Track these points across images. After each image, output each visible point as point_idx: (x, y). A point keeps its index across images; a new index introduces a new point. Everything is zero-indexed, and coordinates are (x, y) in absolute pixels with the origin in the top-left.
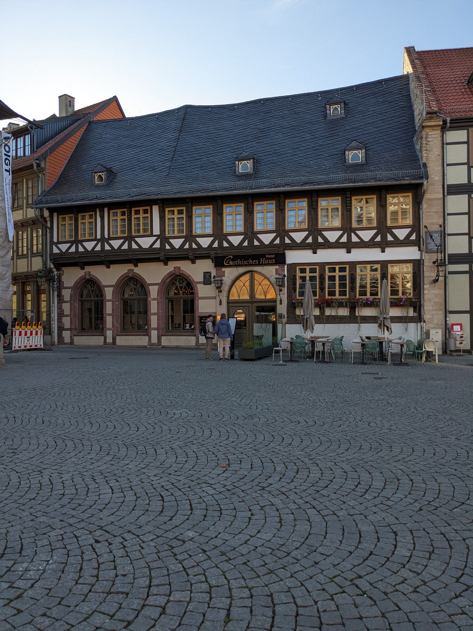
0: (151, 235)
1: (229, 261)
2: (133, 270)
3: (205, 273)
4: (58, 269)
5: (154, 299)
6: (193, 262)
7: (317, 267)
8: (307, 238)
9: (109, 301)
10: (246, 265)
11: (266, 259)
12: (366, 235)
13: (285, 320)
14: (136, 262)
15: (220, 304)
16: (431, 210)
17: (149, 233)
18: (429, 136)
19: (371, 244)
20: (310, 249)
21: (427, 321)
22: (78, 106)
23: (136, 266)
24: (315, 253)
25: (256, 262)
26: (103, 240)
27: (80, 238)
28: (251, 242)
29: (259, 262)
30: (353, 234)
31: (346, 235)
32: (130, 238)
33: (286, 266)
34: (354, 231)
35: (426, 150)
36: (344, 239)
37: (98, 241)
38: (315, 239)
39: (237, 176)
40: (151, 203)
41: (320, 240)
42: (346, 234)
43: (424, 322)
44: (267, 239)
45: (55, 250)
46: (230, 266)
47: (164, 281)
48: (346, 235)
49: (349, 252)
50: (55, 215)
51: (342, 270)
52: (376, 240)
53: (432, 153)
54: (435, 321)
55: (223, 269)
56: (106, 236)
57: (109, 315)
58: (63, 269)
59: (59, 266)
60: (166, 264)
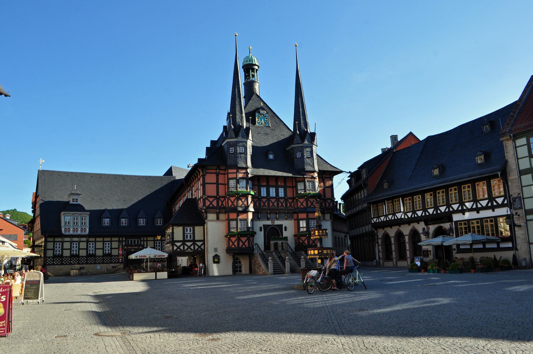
0: (401, 212)
2: (399, 229)
3: (423, 228)
4: (376, 230)
5: (407, 243)
6: (419, 223)
7: (493, 219)
8: (458, 207)
9: (393, 244)
11: (444, 219)
12: (484, 203)
13: (456, 251)
14: (399, 225)
16: (513, 186)
17: (399, 211)
18: (507, 145)
19: (486, 208)
20: (460, 213)
21: (519, 249)
22: (399, 139)
23: (400, 227)
26: (386, 216)
27: (379, 215)
28: (437, 212)
30: (478, 203)
31: (475, 204)
32: (394, 214)
33: (453, 223)
34: (478, 201)
35: (506, 153)
37: (385, 216)
38: (462, 208)
39: (434, 177)
40: (398, 197)
41: (465, 208)
42: (475, 203)
43: (517, 250)
44: (443, 209)
45: (373, 222)
47: (410, 233)
48: (475, 204)
49: (478, 212)
50: (371, 205)
51: (477, 223)
52: (489, 205)
53: (510, 153)
54: (523, 249)
55: (429, 226)
56: (387, 214)
57: (394, 251)
58: (378, 230)
59: (376, 229)
60: (409, 225)
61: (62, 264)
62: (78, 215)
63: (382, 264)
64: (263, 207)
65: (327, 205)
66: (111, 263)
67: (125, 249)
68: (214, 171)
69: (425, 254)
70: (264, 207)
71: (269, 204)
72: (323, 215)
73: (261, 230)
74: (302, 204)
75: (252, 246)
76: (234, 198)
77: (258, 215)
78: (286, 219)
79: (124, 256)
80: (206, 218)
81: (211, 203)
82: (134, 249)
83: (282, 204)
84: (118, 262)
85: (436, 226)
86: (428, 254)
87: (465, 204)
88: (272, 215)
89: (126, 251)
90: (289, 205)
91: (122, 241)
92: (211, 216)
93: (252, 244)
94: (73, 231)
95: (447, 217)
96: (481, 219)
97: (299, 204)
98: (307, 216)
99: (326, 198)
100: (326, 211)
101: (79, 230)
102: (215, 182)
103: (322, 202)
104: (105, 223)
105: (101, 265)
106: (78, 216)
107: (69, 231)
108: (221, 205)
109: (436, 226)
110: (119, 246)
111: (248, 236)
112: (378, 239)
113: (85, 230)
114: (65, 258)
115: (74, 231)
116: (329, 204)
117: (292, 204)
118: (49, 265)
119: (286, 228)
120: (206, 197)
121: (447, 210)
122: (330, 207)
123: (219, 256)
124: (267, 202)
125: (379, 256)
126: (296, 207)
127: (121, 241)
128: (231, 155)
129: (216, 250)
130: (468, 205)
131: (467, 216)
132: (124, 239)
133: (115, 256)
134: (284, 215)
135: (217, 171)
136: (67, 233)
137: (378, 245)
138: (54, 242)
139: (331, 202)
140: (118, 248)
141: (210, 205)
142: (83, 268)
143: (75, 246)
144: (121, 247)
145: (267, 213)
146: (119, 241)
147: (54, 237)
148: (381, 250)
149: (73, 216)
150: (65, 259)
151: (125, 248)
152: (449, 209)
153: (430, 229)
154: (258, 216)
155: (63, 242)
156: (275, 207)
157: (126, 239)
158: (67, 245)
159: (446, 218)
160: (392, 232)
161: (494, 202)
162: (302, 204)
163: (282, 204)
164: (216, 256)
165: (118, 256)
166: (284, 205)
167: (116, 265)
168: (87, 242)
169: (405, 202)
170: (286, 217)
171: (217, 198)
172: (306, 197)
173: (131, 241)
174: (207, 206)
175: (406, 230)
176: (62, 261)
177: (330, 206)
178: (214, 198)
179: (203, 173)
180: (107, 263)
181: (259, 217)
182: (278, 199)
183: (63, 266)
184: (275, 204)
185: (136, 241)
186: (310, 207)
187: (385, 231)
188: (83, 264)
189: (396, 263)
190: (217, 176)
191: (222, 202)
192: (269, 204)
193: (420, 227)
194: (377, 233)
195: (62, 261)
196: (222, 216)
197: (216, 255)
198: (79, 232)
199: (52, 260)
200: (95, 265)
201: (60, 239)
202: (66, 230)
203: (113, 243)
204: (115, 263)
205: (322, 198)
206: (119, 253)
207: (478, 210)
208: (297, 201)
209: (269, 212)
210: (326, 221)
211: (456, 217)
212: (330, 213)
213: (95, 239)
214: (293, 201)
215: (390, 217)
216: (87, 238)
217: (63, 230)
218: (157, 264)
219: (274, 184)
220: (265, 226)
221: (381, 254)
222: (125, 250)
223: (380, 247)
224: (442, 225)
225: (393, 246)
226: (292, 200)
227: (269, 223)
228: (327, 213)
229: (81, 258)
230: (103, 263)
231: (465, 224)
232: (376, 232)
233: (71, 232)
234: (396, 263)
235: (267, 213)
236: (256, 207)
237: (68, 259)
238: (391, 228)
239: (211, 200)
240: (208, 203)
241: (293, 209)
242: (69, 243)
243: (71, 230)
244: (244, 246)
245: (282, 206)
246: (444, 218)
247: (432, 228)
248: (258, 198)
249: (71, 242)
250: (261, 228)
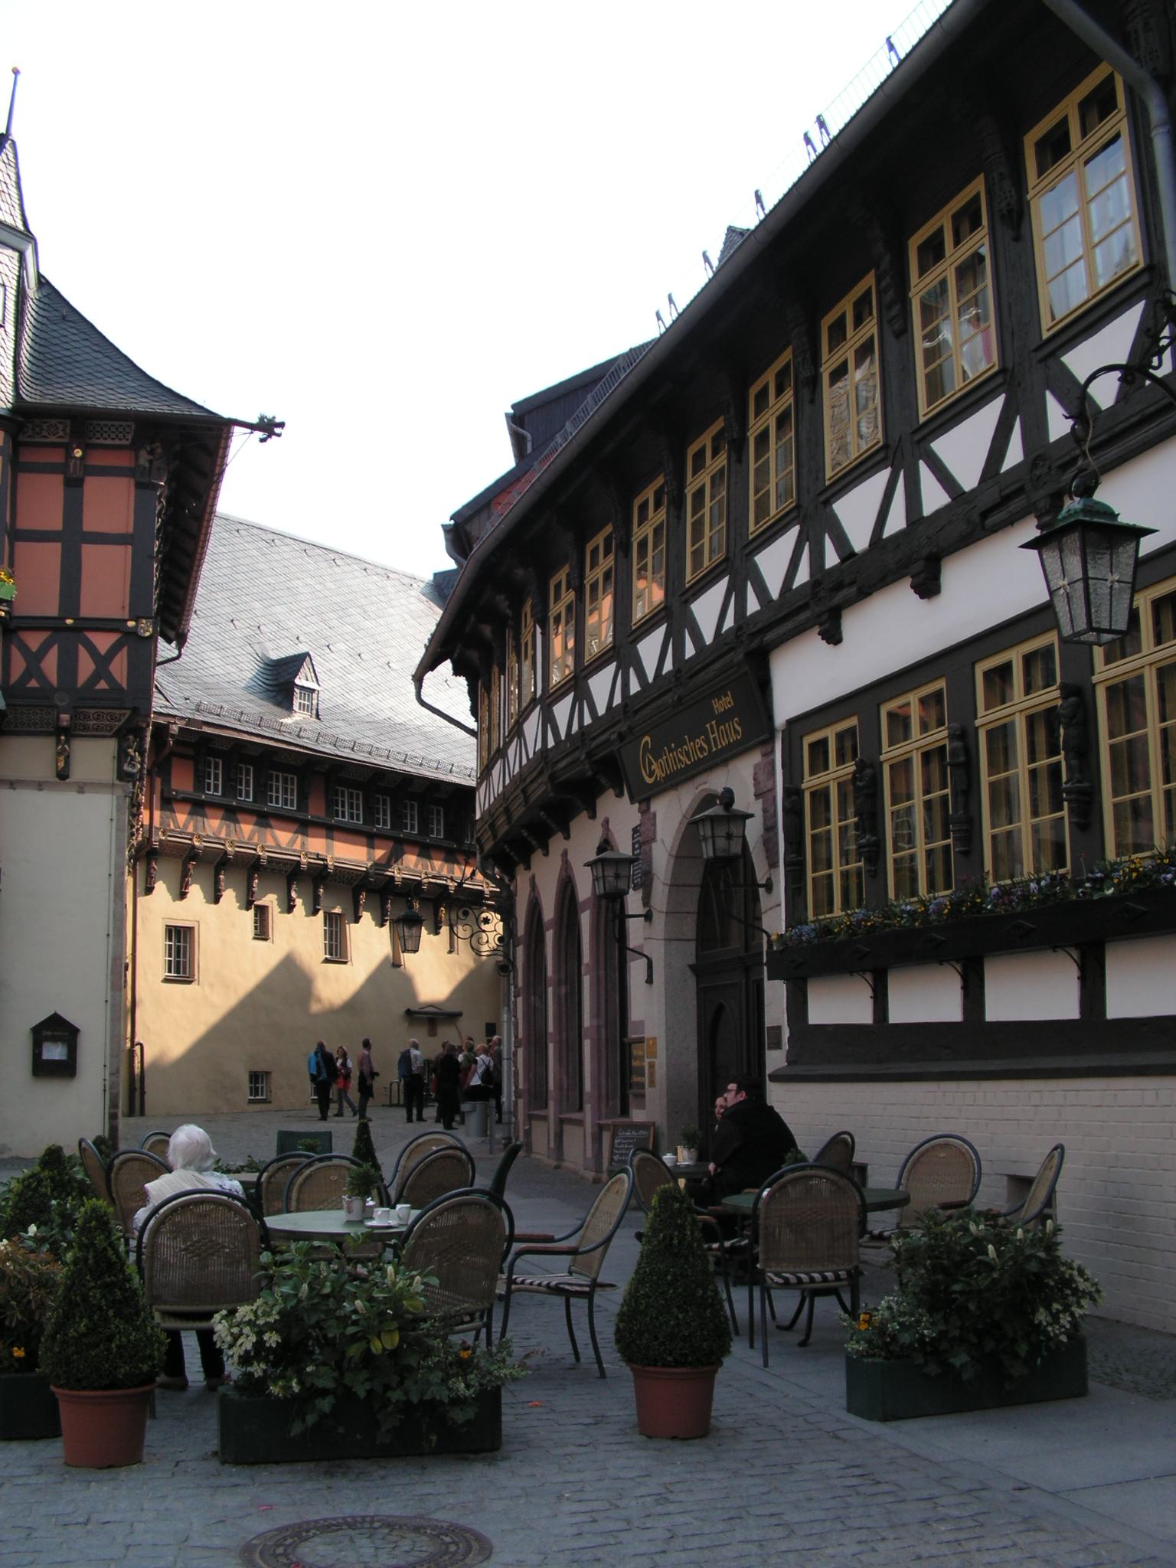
24: (833, 637)
49: (928, 587)
65: (86, 667)
103: (45, 648)
116: (103, 662)
122: (103, 685)
139: (114, 650)
153: (659, 837)
177: (110, 679)
212: (121, 735)
224: (716, 781)
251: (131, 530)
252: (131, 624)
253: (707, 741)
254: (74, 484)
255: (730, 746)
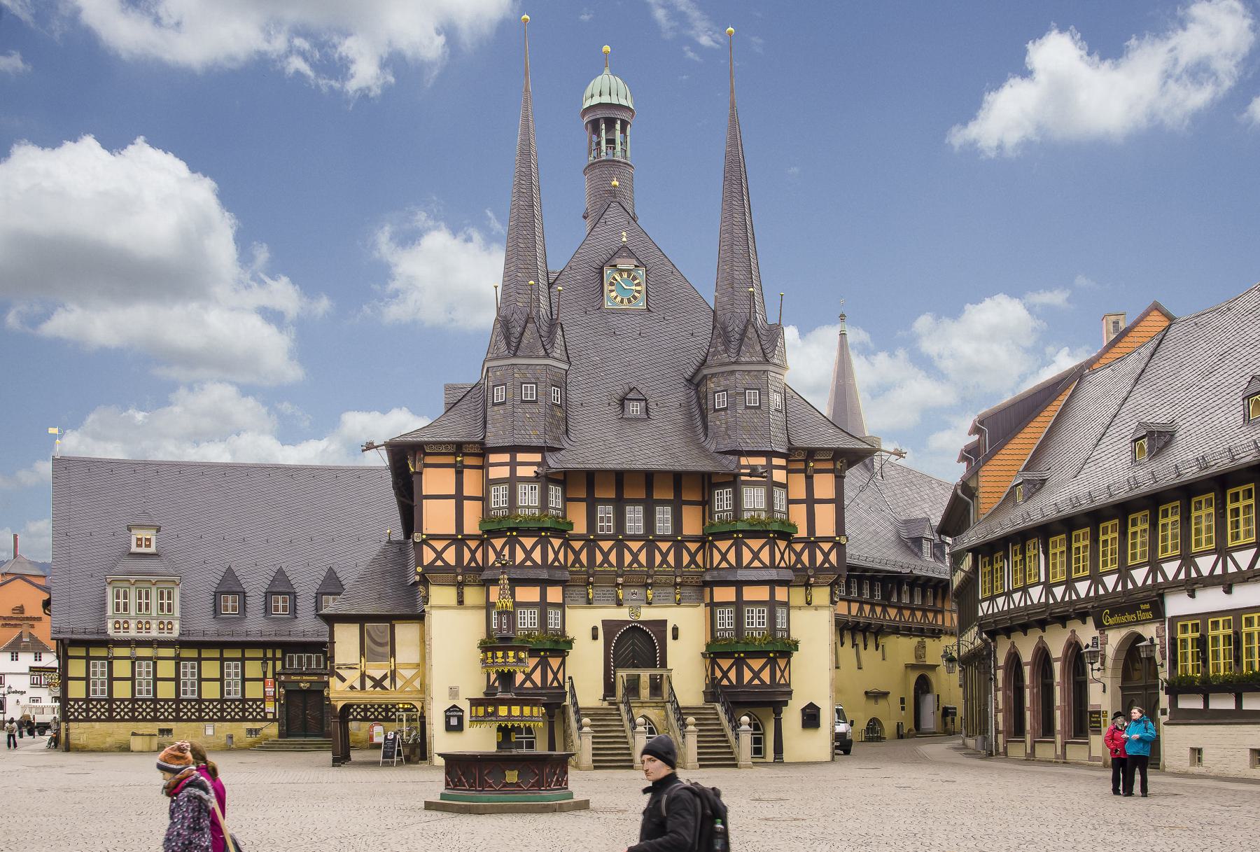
1: (1108, 618)
3: (1094, 638)
10: (1125, 623)
15: (1104, 691)
24: (1192, 595)
25: (1133, 618)
29: (1136, 616)
36: (1218, 571)
38: (1188, 573)
44: (1139, 575)
46: (1110, 627)
49: (1228, 591)
61: (111, 719)
62: (148, 585)
63: (1001, 750)
64: (601, 565)
65: (820, 558)
66: (243, 719)
67: (283, 682)
68: (450, 460)
69: (1094, 722)
70: (606, 565)
71: (620, 557)
72: (807, 589)
73: (595, 637)
74: (724, 557)
75: (555, 684)
76: (503, 540)
77: (587, 590)
78: (679, 603)
79: (279, 700)
80: (426, 599)
81: (439, 555)
82: (307, 682)
83: (665, 556)
84: (264, 719)
85: (1124, 632)
86: (1100, 722)
87: (1197, 560)
88: (632, 591)
89: (284, 688)
90: (686, 559)
91: (274, 659)
92: (441, 595)
93: (555, 678)
94: (138, 629)
95: (1152, 601)
96: (1237, 613)
97: (717, 557)
98: (739, 594)
99: (815, 538)
100: (812, 579)
101: (154, 626)
102: (453, 492)
104: (227, 606)
105: (217, 724)
106: (129, 588)
107: (128, 628)
108: (470, 562)
109: (1124, 632)
110: (265, 673)
111: (542, 653)
112: (996, 668)
113: (170, 627)
114: (162, 703)
115: (141, 628)
116: (826, 555)
117: (699, 558)
118: (76, 720)
119: (675, 629)
120: (424, 537)
121: (1149, 582)
122: (827, 565)
123: (462, 711)
124: (614, 551)
125: (997, 723)
126: (708, 567)
127: (269, 659)
128: (496, 408)
129: (454, 692)
130: (1205, 564)
131: (1211, 600)
132: (279, 655)
133: (254, 701)
134: (671, 590)
135: (459, 459)
136: (122, 635)
137: (997, 690)
138: (88, 658)
140: (263, 679)
141: (435, 560)
142: (169, 731)
143: (144, 669)
144: (270, 675)
145: (617, 585)
146: (265, 660)
147: (87, 644)
148: (1001, 706)
149: (114, 588)
150: (119, 707)
151: (283, 678)
152: (1188, 573)
154: (588, 594)
155: (110, 661)
156: (640, 565)
157: (284, 655)
158: (121, 669)
159: (1147, 606)
160: (1027, 648)
161: (1228, 557)
162: (724, 557)
163: (665, 556)
164: (453, 711)
165: (263, 701)
166: (671, 559)
167: (257, 725)
168: (178, 660)
169: (1051, 551)
170: (678, 597)
171: (458, 540)
172: (735, 535)
173: (300, 659)
174: (425, 564)
175: (1057, 643)
176: (111, 710)
177: (830, 563)
178: (446, 542)
179: (414, 466)
180: (233, 720)
181: (590, 597)
182: (653, 541)
183: (115, 724)
184: (643, 558)
185: (305, 660)
186: (748, 567)
187: (1013, 644)
188: (166, 720)
189: (1033, 748)
190: (459, 474)
191: (473, 552)
192: (620, 557)
193: (1086, 633)
194: (995, 647)
195: (155, 710)
196: (473, 595)
197: (454, 706)
198: (154, 633)
199: (84, 706)
200: (201, 724)
201: (102, 652)
202: (117, 626)
203: (218, 663)
204: (254, 720)
205: (796, 536)
206: (265, 692)
207: (1227, 583)
208: (712, 546)
209: (620, 580)
210: (816, 610)
211: (1177, 605)
212: (831, 585)
213: (200, 654)
214: (702, 547)
215: (1017, 596)
216: (175, 648)
217: (110, 625)
218: (372, 727)
219: (642, 495)
220: (609, 625)
221: (1000, 716)
222: (282, 684)
223: (1000, 694)
224: (1139, 629)
225: (1027, 692)
226: (697, 545)
227: (622, 614)
228: (817, 585)
229: (162, 703)
230: (222, 719)
231: (1228, 624)
232: (992, 644)
233: (133, 633)
234: (1033, 748)
235: (589, 583)
236: (577, 565)
237: (170, 707)
238: (1026, 634)
239: (439, 545)
240: (428, 556)
241: (701, 575)
242: (128, 663)
243: (133, 624)
244: (528, 684)
245: (664, 561)
246: (1142, 606)
247: (1114, 638)
248: (586, 540)
249: (134, 660)
250: (595, 629)
251: (834, 497)
252: (837, 538)
253: (1136, 616)
254: (809, 479)
255: (1146, 620)
